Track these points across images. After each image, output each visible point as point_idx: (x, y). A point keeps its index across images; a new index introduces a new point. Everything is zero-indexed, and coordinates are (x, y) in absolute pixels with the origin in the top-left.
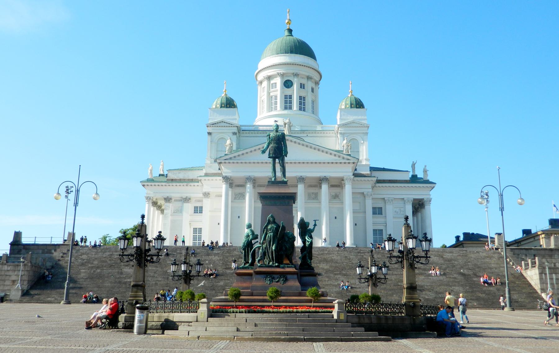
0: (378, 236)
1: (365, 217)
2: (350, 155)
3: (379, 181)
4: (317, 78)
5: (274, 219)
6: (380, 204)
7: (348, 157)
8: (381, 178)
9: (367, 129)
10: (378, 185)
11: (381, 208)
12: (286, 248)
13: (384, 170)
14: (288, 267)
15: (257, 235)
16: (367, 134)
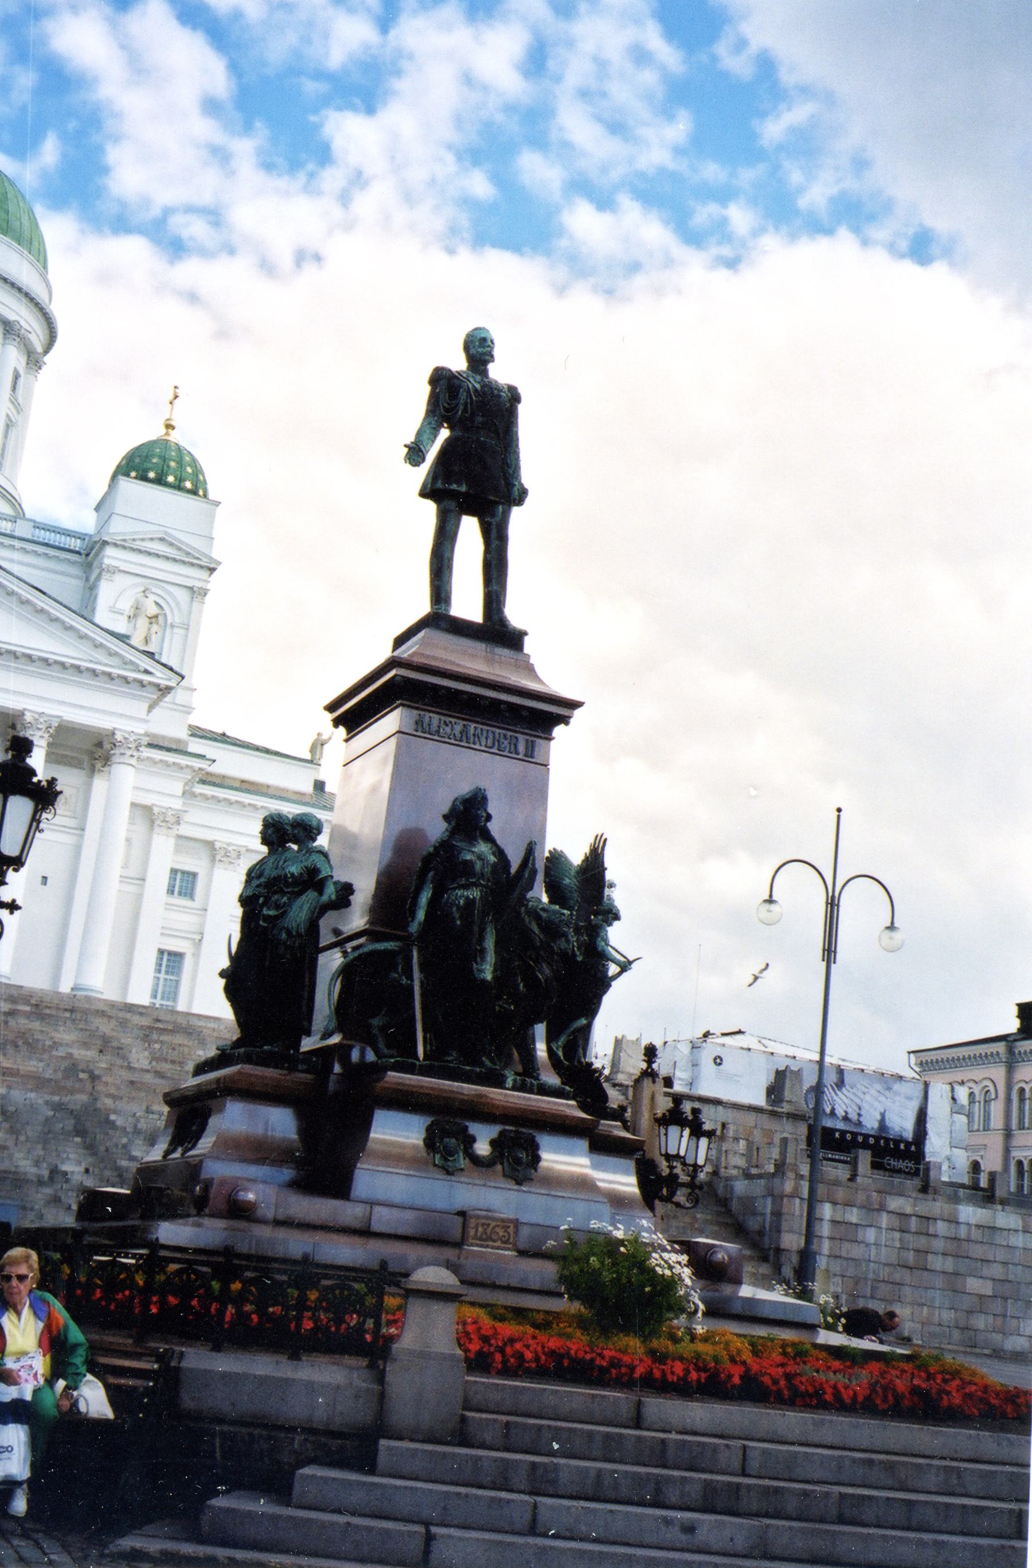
0: (162, 976)
1: (140, 896)
2: (151, 655)
3: (208, 780)
4: (37, 342)
5: (489, 817)
6: (188, 864)
7: (146, 663)
8: (215, 769)
9: (203, 574)
10: (200, 789)
11: (194, 875)
12: (531, 981)
13: (223, 738)
14: (544, 1090)
15: (346, 890)
16: (204, 592)
